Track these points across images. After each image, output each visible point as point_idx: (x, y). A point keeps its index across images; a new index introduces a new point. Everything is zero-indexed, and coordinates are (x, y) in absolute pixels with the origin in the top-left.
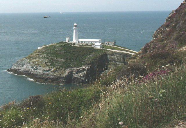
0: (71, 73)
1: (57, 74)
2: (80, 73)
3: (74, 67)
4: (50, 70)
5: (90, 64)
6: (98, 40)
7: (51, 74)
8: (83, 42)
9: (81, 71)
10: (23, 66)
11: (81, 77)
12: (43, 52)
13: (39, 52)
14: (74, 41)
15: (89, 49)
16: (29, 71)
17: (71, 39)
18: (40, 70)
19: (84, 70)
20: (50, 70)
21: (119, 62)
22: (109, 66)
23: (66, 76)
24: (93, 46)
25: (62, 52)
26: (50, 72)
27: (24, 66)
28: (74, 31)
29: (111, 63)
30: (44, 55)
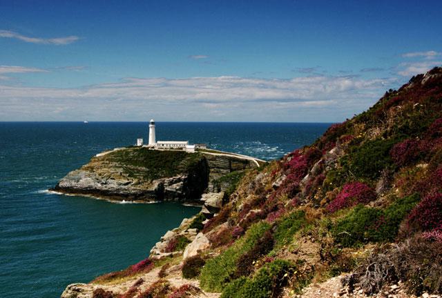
0: (161, 186)
1: (141, 187)
2: (175, 185)
3: (165, 177)
4: (130, 183)
5: (186, 172)
6: (186, 142)
7: (132, 189)
8: (165, 146)
9: (176, 182)
10: (78, 181)
11: (177, 190)
12: (111, 160)
13: (103, 160)
14: (152, 143)
15: (181, 154)
16: (90, 187)
17: (146, 142)
18: (113, 185)
19: (179, 180)
20: (130, 183)
21: (223, 168)
22: (210, 174)
23: (155, 190)
24: (184, 150)
25: (141, 159)
26: (129, 185)
27: (81, 181)
28: (151, 130)
29: (212, 170)
30: (114, 163)
